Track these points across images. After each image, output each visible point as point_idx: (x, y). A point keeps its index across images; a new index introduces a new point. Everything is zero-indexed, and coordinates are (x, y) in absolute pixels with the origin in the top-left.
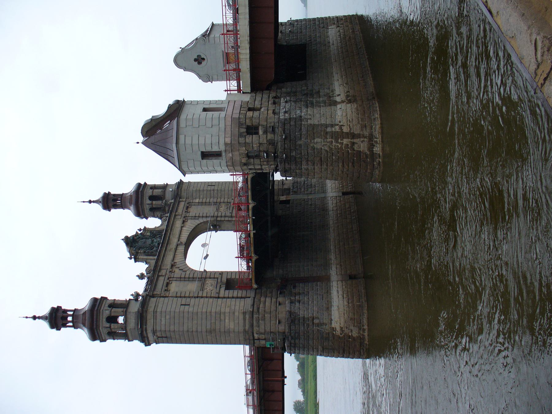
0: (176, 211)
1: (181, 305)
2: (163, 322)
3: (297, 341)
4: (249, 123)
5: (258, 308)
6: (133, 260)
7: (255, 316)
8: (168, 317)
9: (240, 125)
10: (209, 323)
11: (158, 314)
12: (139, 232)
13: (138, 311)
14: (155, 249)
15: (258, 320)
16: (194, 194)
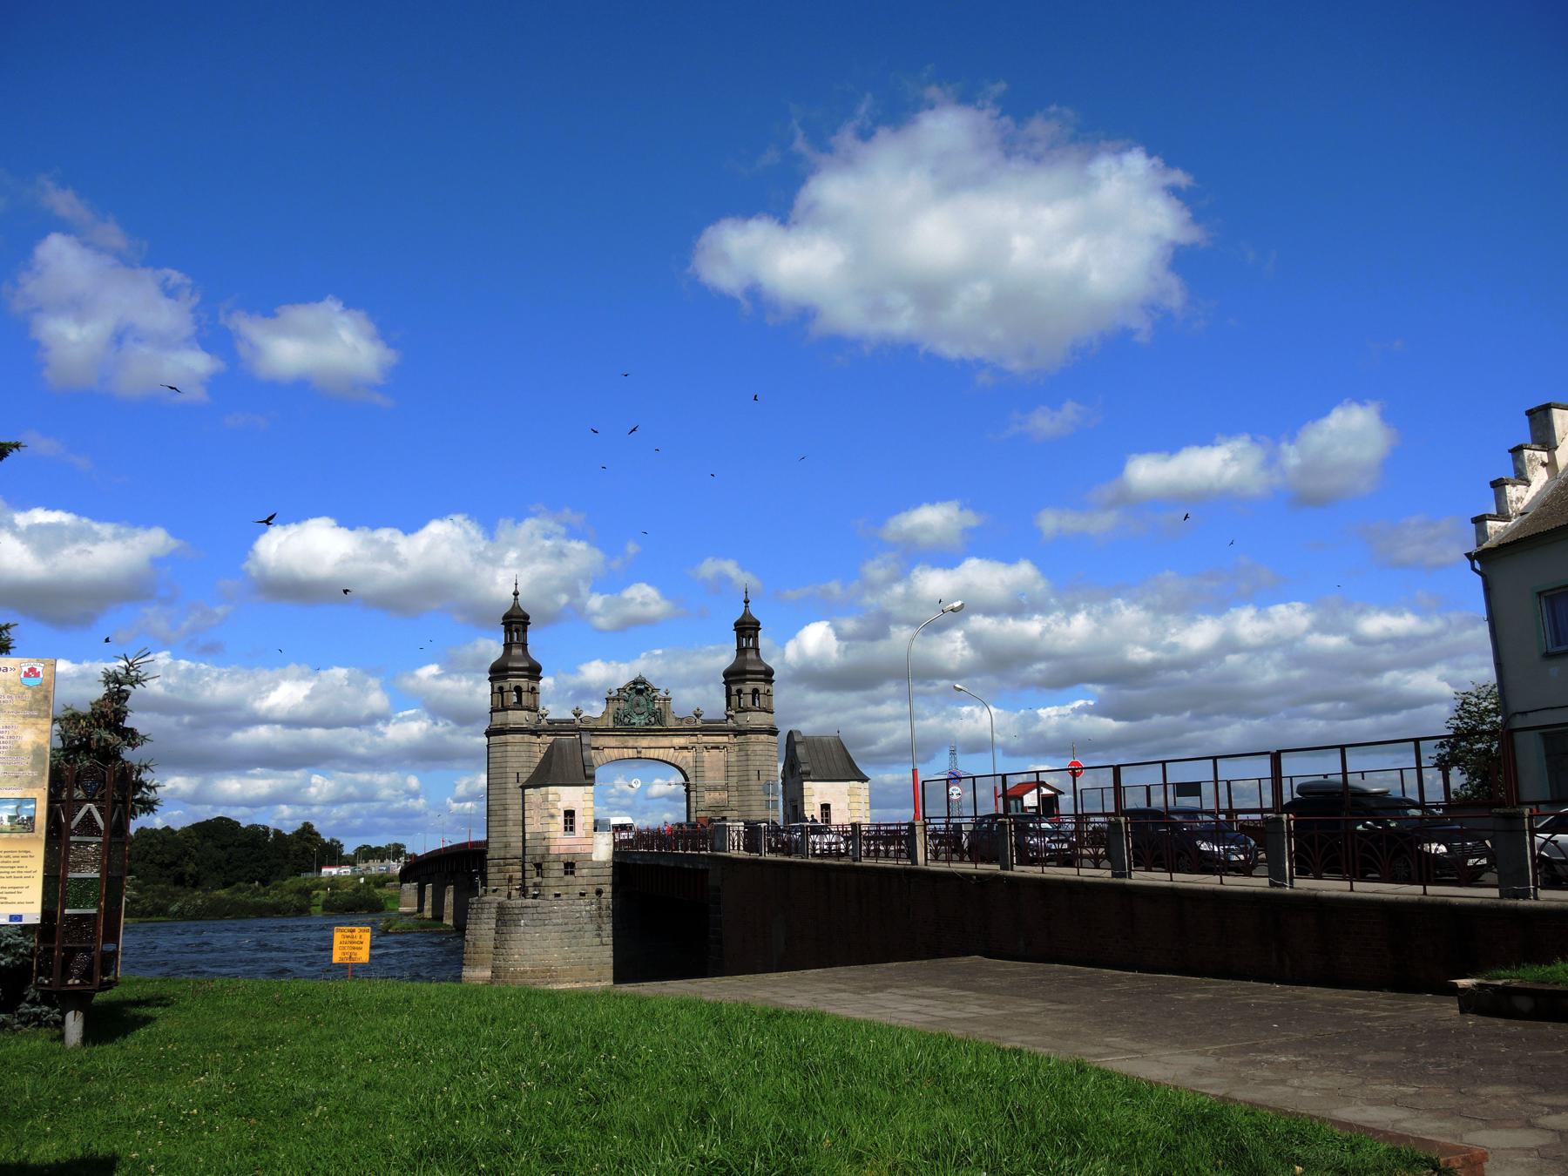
0: (704, 735)
1: (518, 774)
2: (499, 755)
3: (475, 910)
4: (545, 865)
5: (512, 865)
6: (608, 695)
7: (502, 861)
8: (502, 760)
9: (543, 856)
10: (496, 808)
11: (503, 749)
12: (662, 694)
13: (506, 724)
14: (626, 720)
15: (498, 865)
16: (742, 753)
